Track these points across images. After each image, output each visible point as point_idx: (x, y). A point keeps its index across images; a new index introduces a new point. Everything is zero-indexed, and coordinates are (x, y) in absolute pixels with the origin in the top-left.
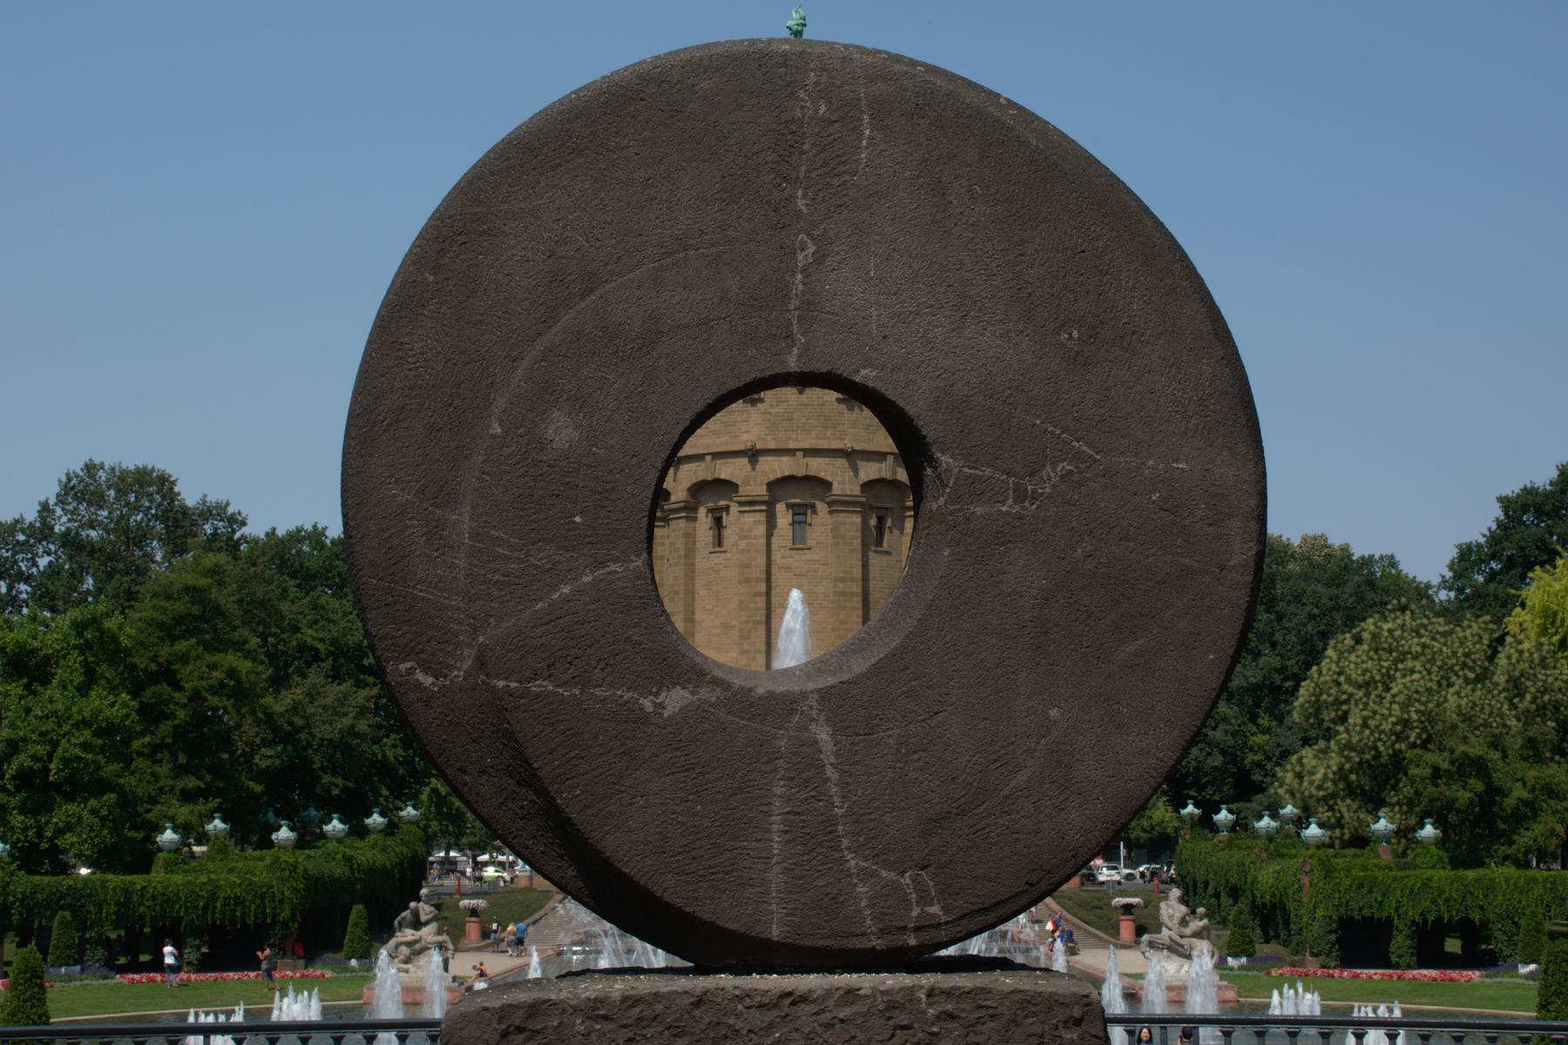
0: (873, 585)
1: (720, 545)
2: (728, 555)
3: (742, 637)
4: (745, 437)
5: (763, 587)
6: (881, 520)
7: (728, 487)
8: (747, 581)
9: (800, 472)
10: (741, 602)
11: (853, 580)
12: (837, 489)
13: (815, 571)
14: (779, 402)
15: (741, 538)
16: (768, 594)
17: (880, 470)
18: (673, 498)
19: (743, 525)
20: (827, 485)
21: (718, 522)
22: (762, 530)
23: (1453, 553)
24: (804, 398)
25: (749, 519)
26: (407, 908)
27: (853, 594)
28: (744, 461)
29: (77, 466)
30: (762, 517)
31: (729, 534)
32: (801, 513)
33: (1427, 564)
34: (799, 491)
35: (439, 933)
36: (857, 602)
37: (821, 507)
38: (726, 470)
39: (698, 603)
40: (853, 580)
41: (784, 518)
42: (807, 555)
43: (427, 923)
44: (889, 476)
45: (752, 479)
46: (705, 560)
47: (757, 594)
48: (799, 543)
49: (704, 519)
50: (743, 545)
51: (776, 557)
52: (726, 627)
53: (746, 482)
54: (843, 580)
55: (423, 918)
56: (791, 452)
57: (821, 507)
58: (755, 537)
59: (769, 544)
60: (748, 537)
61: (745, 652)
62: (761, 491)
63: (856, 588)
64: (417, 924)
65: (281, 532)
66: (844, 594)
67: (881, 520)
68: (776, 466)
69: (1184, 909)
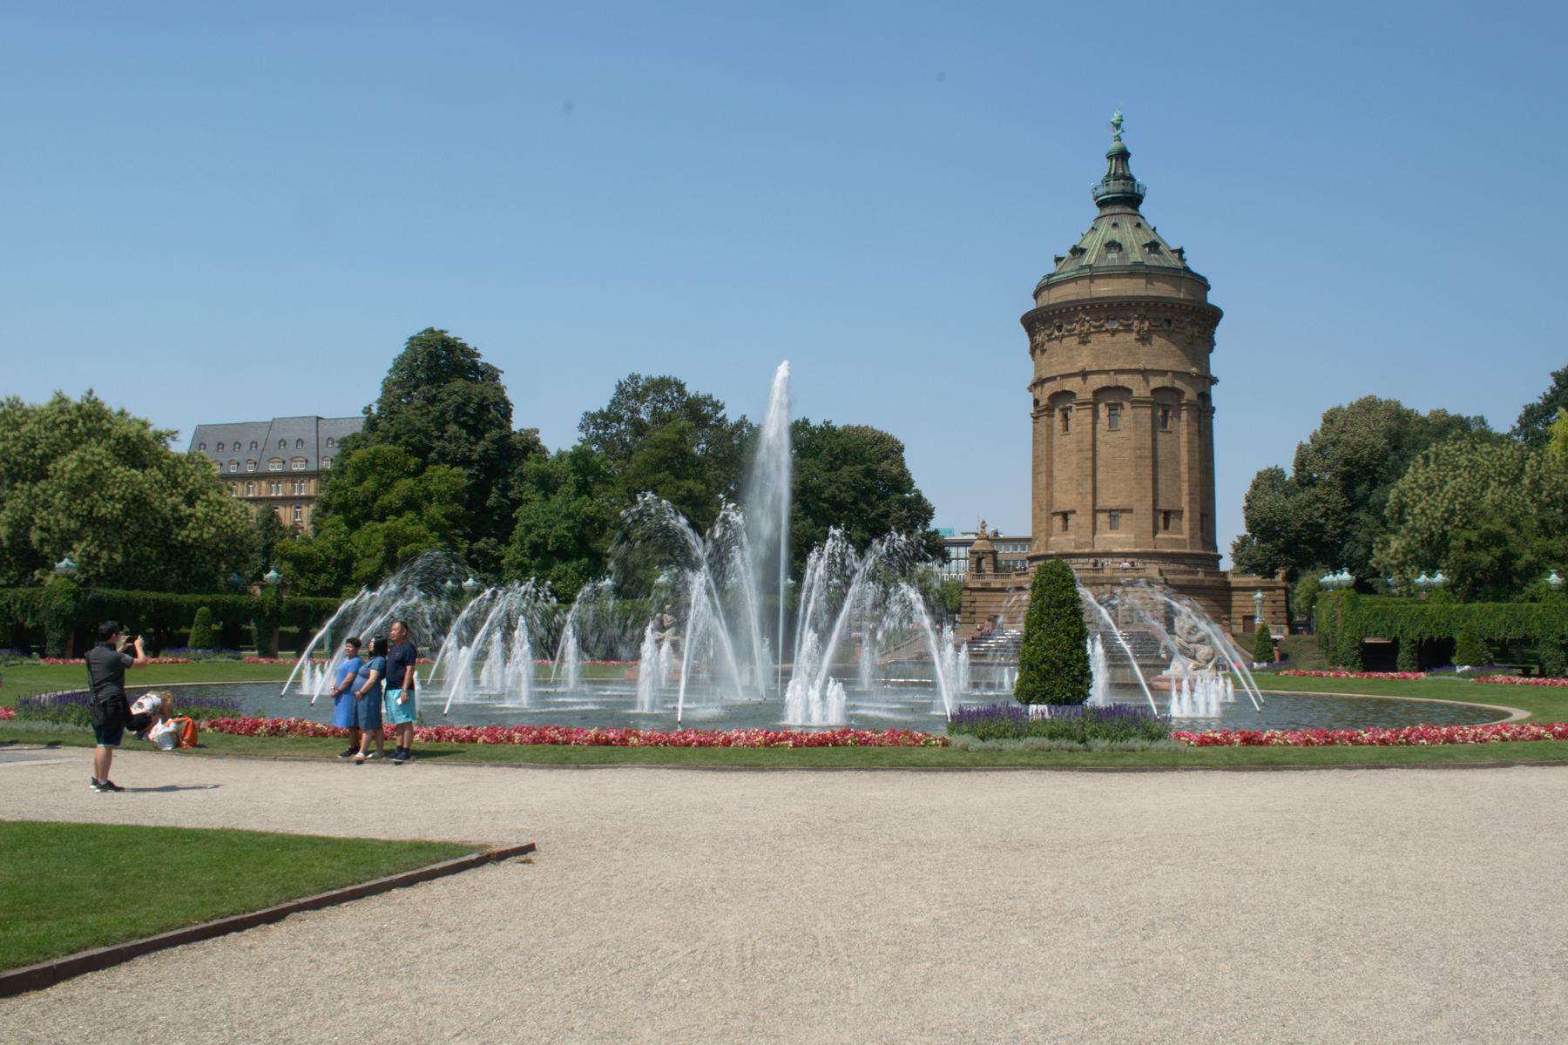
0: (1160, 452)
5: (1090, 454)
6: (1165, 412)
9: (1113, 384)
12: (1135, 393)
16: (1094, 459)
19: (1080, 417)
20: (1130, 391)
22: (1089, 419)
23: (1521, 411)
25: (1082, 413)
28: (1079, 379)
29: (624, 377)
30: (1089, 412)
31: (1072, 423)
32: (1114, 408)
33: (1503, 421)
34: (1112, 396)
36: (1149, 462)
37: (1127, 405)
38: (1069, 385)
41: (1103, 412)
42: (1118, 434)
46: (1058, 439)
48: (1112, 427)
49: (1058, 414)
51: (1099, 436)
52: (1070, 479)
56: (1107, 372)
57: (1127, 405)
59: (1094, 429)
62: (1089, 396)
63: (1148, 453)
67: (1165, 412)
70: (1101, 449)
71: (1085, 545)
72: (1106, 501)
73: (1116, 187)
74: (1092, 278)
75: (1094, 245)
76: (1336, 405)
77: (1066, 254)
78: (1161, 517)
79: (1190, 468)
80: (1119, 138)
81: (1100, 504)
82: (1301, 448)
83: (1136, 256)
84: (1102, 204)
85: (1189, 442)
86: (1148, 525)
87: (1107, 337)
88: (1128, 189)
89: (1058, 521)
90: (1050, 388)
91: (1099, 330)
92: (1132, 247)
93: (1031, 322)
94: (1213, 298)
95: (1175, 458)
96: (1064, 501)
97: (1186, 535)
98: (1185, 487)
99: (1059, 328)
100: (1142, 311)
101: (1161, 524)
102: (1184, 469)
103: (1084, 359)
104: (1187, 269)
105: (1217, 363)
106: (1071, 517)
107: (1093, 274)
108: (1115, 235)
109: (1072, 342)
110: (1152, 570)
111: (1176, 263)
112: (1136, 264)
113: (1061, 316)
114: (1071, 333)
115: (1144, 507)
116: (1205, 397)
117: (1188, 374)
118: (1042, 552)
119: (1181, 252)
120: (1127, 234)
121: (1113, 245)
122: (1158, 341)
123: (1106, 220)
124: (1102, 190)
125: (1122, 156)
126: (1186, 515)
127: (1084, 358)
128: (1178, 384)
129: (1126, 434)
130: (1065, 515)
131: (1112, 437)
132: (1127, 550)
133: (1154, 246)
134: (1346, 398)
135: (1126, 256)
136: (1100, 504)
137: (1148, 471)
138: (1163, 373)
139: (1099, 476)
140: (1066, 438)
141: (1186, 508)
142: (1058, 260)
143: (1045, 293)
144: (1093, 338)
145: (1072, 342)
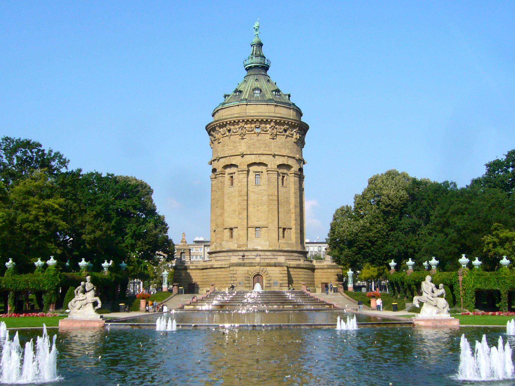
1: (232, 185)
2: (235, 188)
3: (239, 214)
4: (240, 150)
5: (246, 198)
8: (241, 196)
9: (258, 161)
10: (239, 203)
11: (274, 196)
12: (269, 166)
13: (263, 193)
14: (251, 139)
15: (239, 182)
16: (247, 200)
17: (283, 161)
18: (217, 171)
19: (240, 178)
20: (266, 165)
22: (246, 179)
24: (259, 138)
26: (80, 285)
27: (275, 200)
31: (235, 181)
32: (258, 174)
35: (95, 296)
36: (276, 202)
39: (225, 204)
40: (274, 196)
42: (260, 188)
43: (89, 291)
44: (286, 163)
47: (245, 200)
50: (239, 184)
53: (241, 164)
54: (271, 195)
55: (87, 289)
58: (244, 182)
59: (247, 185)
60: (241, 182)
61: (241, 218)
62: (246, 168)
63: (276, 198)
64: (84, 292)
65: (84, 172)
66: (272, 200)
68: (250, 159)
69: (433, 285)
70: (251, 195)
71: (244, 245)
72: (254, 222)
73: (256, 61)
75: (246, 88)
76: (376, 174)
77: (230, 92)
78: (281, 230)
79: (295, 206)
81: (250, 224)
83: (269, 96)
85: (295, 193)
88: (262, 61)
89: (227, 233)
90: (223, 162)
92: (267, 92)
93: (211, 129)
94: (303, 119)
95: (288, 202)
96: (231, 222)
97: (294, 240)
98: (293, 216)
99: (229, 131)
100: (273, 124)
101: (281, 235)
102: (292, 206)
103: (243, 148)
104: (294, 104)
105: (307, 153)
106: (235, 230)
107: (248, 102)
108: (257, 85)
109: (237, 138)
110: (281, 259)
111: (287, 101)
112: (270, 99)
113: (230, 123)
115: (273, 226)
116: (301, 170)
117: (294, 158)
118: (218, 249)
119: (289, 96)
120: (262, 84)
122: (281, 139)
123: (251, 77)
124: (250, 61)
125: (260, 45)
126: (293, 230)
128: (291, 162)
129: (262, 188)
130: (231, 229)
131: (257, 189)
132: (265, 249)
133: (278, 91)
134: (381, 170)
135: (263, 96)
136: (250, 224)
139: (250, 209)
140: (232, 189)
141: (293, 227)
143: (217, 114)
145: (236, 138)
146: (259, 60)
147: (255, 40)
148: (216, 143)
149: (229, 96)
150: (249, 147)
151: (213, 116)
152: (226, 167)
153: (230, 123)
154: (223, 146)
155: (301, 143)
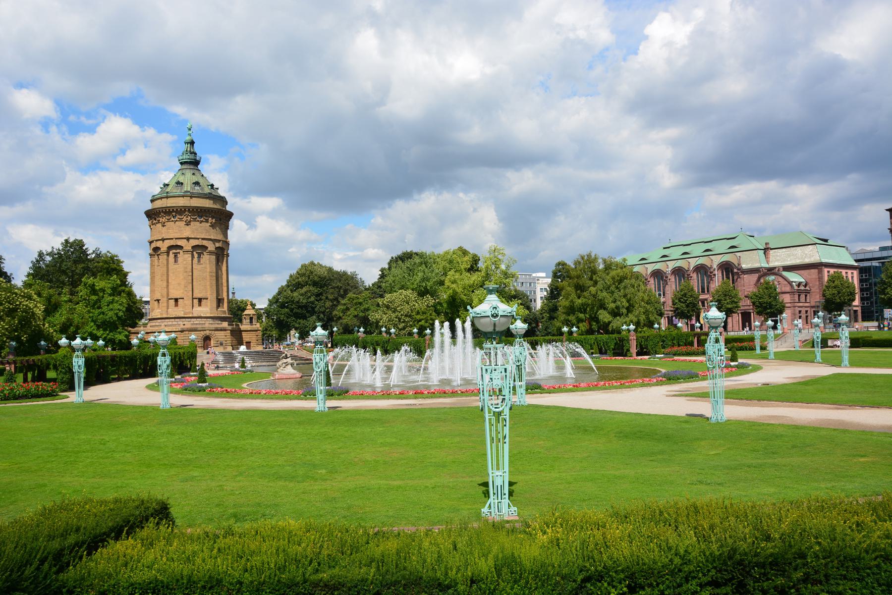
7: (181, 247)
20: (207, 248)
21: (176, 256)
31: (180, 259)
32: (199, 255)
34: (199, 249)
38: (179, 243)
41: (196, 255)
45: (188, 246)
49: (172, 255)
52: (179, 284)
62: (190, 249)
71: (189, 313)
72: (197, 294)
74: (191, 197)
80: (190, 135)
82: (291, 276)
83: (207, 190)
84: (181, 163)
86: (215, 305)
87: (198, 223)
89: (172, 302)
90: (168, 243)
91: (195, 220)
93: (152, 215)
103: (187, 232)
108: (195, 179)
110: (225, 324)
113: (177, 212)
114: (181, 220)
115: (212, 298)
121: (197, 183)
123: (188, 171)
125: (192, 143)
127: (187, 232)
130: (176, 300)
131: (199, 267)
133: (212, 186)
135: (202, 189)
137: (214, 282)
138: (219, 241)
140: (176, 266)
142: (166, 185)
144: (192, 223)
146: (192, 156)
147: (188, 138)
148: (159, 225)
149: (168, 185)
150: (193, 232)
151: (152, 201)
152: (170, 248)
153: (177, 212)
154: (168, 229)
155: (225, 228)
